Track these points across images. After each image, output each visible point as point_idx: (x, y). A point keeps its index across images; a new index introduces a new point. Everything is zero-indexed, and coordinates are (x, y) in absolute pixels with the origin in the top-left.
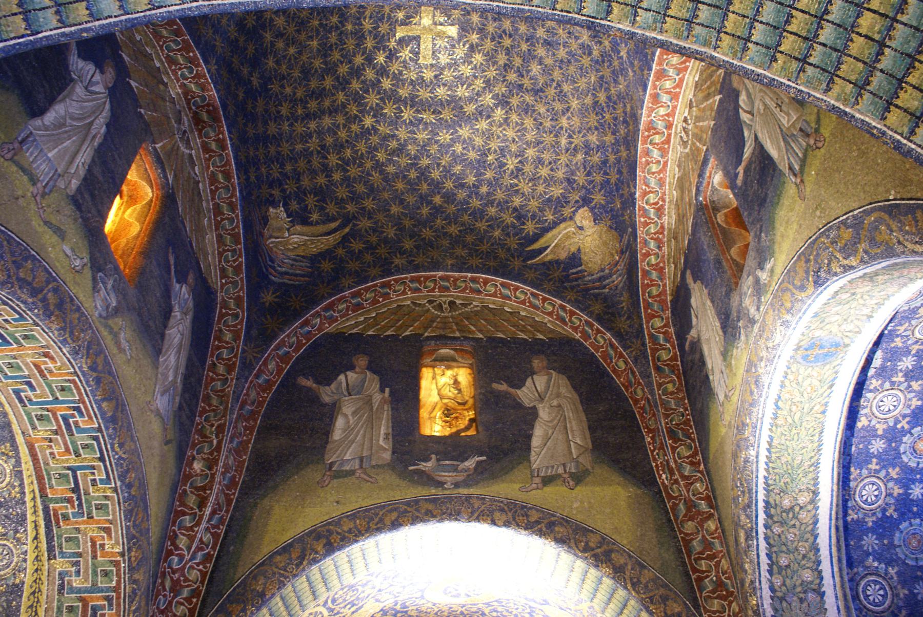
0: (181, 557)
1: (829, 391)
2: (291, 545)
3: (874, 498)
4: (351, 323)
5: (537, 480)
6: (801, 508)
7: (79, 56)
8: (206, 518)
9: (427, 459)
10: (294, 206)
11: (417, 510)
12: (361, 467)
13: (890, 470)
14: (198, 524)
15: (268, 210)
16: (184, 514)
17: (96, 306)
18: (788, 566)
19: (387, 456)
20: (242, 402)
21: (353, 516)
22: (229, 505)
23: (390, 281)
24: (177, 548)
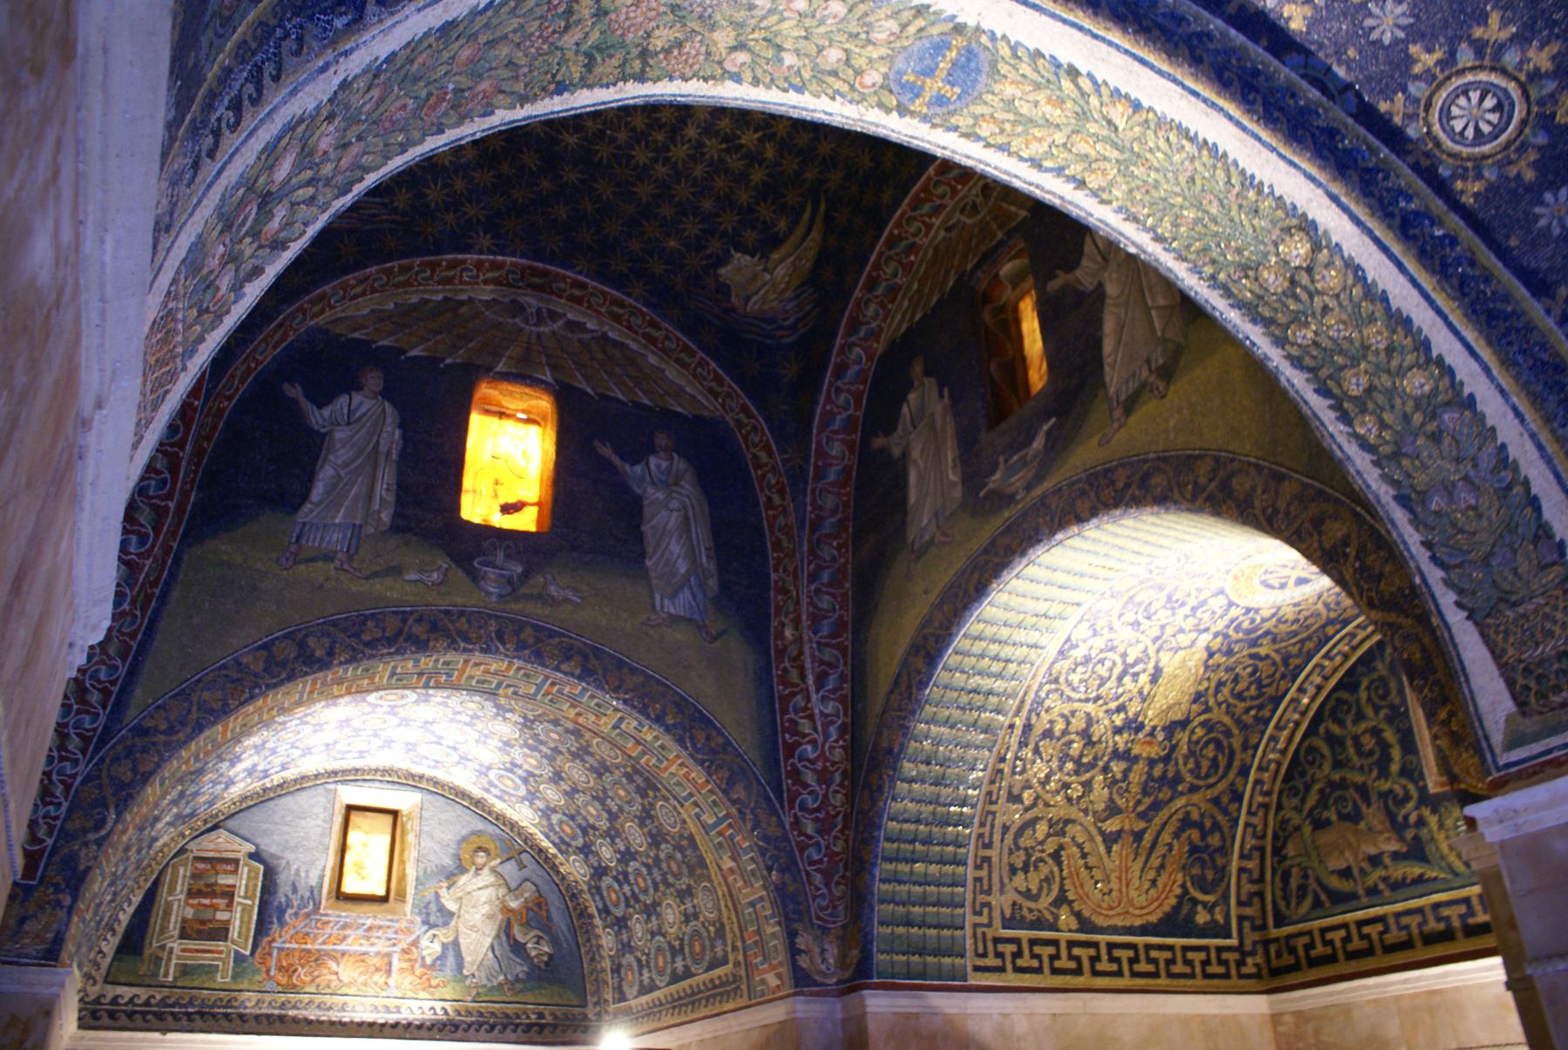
0: (814, 742)
1: (1080, 80)
2: (899, 676)
3: (1494, 118)
4: (897, 323)
5: (1118, 413)
6: (1309, 270)
7: (320, 407)
8: (812, 688)
9: (993, 473)
10: (750, 236)
11: (996, 554)
12: (938, 528)
13: (1478, 32)
14: (808, 700)
15: (717, 276)
16: (794, 694)
17: (489, 594)
18: (1370, 389)
19: (957, 493)
20: (813, 523)
21: (939, 606)
22: (845, 656)
23: (891, 233)
24: (804, 736)
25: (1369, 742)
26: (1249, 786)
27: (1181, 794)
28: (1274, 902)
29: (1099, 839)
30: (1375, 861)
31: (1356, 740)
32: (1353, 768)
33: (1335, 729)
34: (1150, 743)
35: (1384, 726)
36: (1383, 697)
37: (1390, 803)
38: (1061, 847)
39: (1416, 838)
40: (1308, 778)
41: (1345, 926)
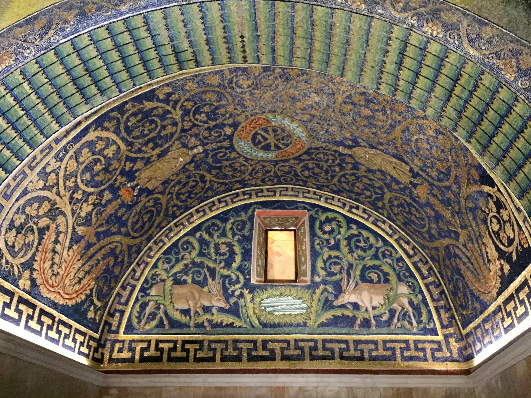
25: (224, 249)
26: (146, 248)
27: (120, 234)
28: (130, 319)
29: (69, 236)
30: (207, 310)
31: (217, 246)
32: (210, 259)
33: (206, 237)
34: (130, 193)
35: (235, 243)
36: (240, 230)
37: (227, 282)
38: (48, 228)
39: (236, 304)
40: (180, 256)
41: (175, 342)
